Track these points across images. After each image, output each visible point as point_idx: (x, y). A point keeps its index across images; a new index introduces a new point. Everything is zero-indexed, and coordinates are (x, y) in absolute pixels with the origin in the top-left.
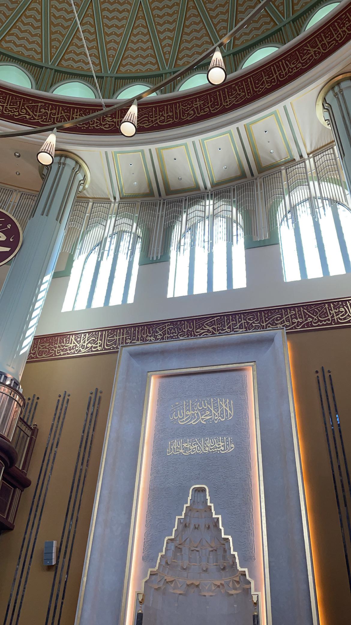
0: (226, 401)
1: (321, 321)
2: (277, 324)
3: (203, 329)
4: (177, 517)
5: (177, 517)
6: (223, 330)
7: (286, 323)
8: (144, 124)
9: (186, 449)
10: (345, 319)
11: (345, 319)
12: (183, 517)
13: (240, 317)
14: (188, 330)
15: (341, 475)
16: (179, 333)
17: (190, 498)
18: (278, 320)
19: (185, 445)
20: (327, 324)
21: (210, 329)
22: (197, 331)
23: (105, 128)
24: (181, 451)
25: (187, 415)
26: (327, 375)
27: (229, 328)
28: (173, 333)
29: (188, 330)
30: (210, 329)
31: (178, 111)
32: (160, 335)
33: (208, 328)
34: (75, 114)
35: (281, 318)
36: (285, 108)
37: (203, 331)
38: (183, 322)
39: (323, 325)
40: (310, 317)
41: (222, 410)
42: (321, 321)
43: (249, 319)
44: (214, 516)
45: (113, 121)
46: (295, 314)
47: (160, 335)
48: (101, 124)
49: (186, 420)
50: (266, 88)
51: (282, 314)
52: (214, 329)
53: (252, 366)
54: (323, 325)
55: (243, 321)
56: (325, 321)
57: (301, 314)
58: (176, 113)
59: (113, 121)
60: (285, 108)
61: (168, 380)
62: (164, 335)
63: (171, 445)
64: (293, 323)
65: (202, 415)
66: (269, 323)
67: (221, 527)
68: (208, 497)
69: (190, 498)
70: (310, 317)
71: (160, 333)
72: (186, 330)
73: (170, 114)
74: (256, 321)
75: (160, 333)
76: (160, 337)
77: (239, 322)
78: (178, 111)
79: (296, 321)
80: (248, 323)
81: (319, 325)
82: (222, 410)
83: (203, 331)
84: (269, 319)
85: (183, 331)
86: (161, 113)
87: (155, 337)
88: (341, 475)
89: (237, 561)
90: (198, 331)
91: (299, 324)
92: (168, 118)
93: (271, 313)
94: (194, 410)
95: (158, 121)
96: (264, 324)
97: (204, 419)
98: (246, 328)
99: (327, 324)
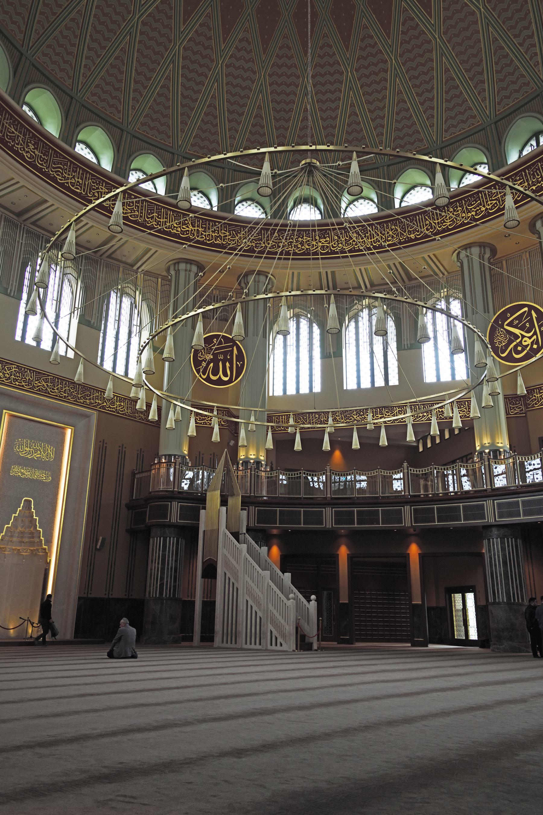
0: (51, 448)
1: (110, 408)
2: (86, 399)
3: (39, 382)
4: (14, 515)
5: (14, 515)
6: (53, 389)
7: (92, 401)
8: (58, 175)
9: (23, 474)
10: (122, 411)
11: (122, 411)
12: (17, 515)
13: (66, 384)
14: (29, 379)
15: (97, 504)
16: (22, 378)
17: (22, 505)
18: (88, 396)
19: (22, 471)
20: (113, 411)
21: (45, 384)
22: (36, 382)
23: (27, 156)
24: (20, 474)
25: (26, 450)
26: (105, 445)
27: (58, 389)
28: (18, 377)
29: (29, 379)
30: (45, 384)
31: (87, 183)
32: (8, 373)
33: (44, 383)
34: (6, 121)
35: (90, 395)
36: (156, 251)
37: (40, 384)
38: (26, 370)
39: (111, 411)
40: (105, 402)
41: (48, 453)
42: (110, 408)
43: (71, 388)
44: (34, 517)
45: (34, 152)
46: (98, 396)
47: (8, 373)
48: (24, 150)
49: (25, 453)
50: (153, 225)
51: (91, 392)
52: (47, 385)
53: (72, 429)
54: (111, 411)
55: (67, 388)
56: (112, 408)
57: (101, 398)
58: (85, 184)
59: (34, 152)
60: (156, 251)
61: (15, 419)
62: (11, 375)
63: (14, 468)
64: (96, 403)
65: (35, 453)
66: (82, 396)
67: (37, 524)
68: (32, 506)
69: (22, 505)
70: (105, 402)
71: (8, 372)
72: (28, 378)
73: (80, 180)
74: (76, 391)
75: (8, 372)
76: (8, 376)
77: (65, 387)
78: (87, 183)
79: (97, 401)
80: (70, 391)
81: (108, 410)
82: (48, 453)
83: (40, 384)
84: (83, 393)
85: (25, 378)
86: (73, 174)
87: (4, 374)
88: (97, 504)
89: (43, 542)
90: (36, 382)
91: (99, 404)
92: (77, 185)
93: (85, 390)
94: (30, 448)
95: (69, 181)
96: (80, 396)
97: (36, 456)
98: (68, 394)
99: (113, 411)
